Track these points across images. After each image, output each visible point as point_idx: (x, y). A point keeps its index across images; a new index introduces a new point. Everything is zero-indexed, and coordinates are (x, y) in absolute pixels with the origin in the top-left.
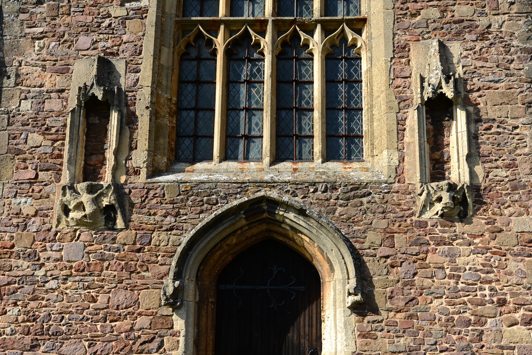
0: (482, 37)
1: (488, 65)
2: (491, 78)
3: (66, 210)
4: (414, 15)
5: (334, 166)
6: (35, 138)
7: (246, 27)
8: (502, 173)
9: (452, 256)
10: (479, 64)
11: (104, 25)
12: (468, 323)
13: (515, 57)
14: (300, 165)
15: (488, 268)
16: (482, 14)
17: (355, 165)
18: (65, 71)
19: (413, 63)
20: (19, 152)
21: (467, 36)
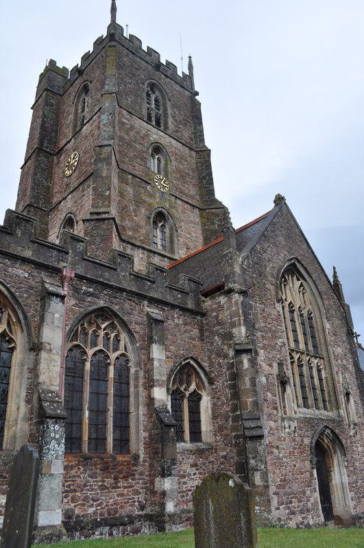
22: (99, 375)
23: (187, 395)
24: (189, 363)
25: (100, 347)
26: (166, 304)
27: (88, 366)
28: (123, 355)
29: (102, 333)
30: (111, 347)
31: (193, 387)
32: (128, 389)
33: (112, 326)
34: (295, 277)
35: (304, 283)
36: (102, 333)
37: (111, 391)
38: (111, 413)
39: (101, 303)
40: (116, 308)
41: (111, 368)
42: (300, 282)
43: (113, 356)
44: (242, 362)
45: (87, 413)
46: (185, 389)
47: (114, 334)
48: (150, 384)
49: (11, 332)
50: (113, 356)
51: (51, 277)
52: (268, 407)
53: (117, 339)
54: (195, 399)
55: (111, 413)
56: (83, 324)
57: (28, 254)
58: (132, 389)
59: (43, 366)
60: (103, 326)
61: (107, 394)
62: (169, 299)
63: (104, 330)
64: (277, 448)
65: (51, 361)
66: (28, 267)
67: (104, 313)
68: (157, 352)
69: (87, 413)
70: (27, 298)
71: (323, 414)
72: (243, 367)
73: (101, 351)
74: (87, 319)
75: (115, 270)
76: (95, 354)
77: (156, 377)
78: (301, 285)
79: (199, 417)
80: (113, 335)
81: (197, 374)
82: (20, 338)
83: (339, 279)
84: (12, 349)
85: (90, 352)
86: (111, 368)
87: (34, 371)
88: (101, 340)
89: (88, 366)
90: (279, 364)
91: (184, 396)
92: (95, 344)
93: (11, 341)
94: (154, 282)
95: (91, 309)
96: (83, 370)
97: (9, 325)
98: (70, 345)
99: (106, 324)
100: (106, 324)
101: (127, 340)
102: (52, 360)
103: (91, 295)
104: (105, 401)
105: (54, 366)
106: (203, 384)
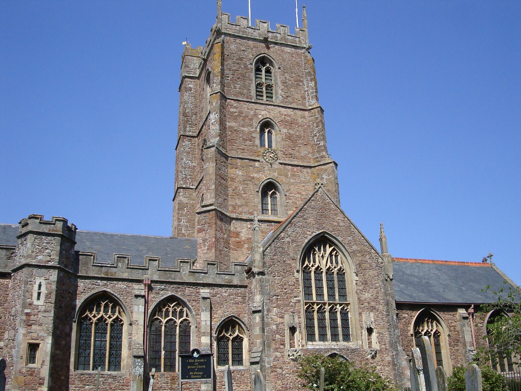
1: (379, 318)
2: (380, 322)
3: (289, 356)
4: (362, 305)
6: (278, 336)
7: (321, 305)
10: (377, 318)
11: (290, 304)
13: (384, 316)
16: (377, 305)
17: (350, 343)
18: (282, 317)
19: (363, 318)
20: (274, 340)
21: (374, 311)
22: (170, 332)
23: (231, 339)
24: (232, 319)
25: (170, 317)
27: (163, 328)
29: (171, 310)
30: (178, 317)
31: (237, 333)
32: (190, 338)
33: (178, 305)
34: (328, 246)
36: (171, 310)
37: (177, 340)
39: (170, 294)
40: (179, 295)
41: (178, 328)
43: (178, 321)
45: (163, 353)
46: (230, 335)
47: (179, 309)
49: (121, 316)
50: (178, 321)
51: (139, 284)
52: (275, 344)
53: (181, 312)
54: (238, 340)
55: (177, 352)
56: (160, 306)
57: (125, 276)
58: (191, 339)
59: (134, 332)
60: (172, 306)
61: (176, 342)
63: (173, 307)
64: (281, 368)
65: (138, 329)
67: (171, 299)
69: (163, 353)
70: (126, 299)
71: (329, 345)
72: (256, 321)
73: (171, 320)
75: (179, 272)
77: (203, 330)
79: (242, 351)
80: (178, 310)
81: (240, 325)
84: (122, 324)
85: (164, 321)
86: (178, 328)
87: (130, 334)
89: (163, 328)
91: (228, 339)
92: (167, 315)
93: (121, 321)
95: (162, 298)
96: (161, 331)
97: (119, 313)
99: (174, 304)
100: (174, 304)
101: (188, 311)
102: (139, 329)
105: (140, 331)
106: (244, 330)
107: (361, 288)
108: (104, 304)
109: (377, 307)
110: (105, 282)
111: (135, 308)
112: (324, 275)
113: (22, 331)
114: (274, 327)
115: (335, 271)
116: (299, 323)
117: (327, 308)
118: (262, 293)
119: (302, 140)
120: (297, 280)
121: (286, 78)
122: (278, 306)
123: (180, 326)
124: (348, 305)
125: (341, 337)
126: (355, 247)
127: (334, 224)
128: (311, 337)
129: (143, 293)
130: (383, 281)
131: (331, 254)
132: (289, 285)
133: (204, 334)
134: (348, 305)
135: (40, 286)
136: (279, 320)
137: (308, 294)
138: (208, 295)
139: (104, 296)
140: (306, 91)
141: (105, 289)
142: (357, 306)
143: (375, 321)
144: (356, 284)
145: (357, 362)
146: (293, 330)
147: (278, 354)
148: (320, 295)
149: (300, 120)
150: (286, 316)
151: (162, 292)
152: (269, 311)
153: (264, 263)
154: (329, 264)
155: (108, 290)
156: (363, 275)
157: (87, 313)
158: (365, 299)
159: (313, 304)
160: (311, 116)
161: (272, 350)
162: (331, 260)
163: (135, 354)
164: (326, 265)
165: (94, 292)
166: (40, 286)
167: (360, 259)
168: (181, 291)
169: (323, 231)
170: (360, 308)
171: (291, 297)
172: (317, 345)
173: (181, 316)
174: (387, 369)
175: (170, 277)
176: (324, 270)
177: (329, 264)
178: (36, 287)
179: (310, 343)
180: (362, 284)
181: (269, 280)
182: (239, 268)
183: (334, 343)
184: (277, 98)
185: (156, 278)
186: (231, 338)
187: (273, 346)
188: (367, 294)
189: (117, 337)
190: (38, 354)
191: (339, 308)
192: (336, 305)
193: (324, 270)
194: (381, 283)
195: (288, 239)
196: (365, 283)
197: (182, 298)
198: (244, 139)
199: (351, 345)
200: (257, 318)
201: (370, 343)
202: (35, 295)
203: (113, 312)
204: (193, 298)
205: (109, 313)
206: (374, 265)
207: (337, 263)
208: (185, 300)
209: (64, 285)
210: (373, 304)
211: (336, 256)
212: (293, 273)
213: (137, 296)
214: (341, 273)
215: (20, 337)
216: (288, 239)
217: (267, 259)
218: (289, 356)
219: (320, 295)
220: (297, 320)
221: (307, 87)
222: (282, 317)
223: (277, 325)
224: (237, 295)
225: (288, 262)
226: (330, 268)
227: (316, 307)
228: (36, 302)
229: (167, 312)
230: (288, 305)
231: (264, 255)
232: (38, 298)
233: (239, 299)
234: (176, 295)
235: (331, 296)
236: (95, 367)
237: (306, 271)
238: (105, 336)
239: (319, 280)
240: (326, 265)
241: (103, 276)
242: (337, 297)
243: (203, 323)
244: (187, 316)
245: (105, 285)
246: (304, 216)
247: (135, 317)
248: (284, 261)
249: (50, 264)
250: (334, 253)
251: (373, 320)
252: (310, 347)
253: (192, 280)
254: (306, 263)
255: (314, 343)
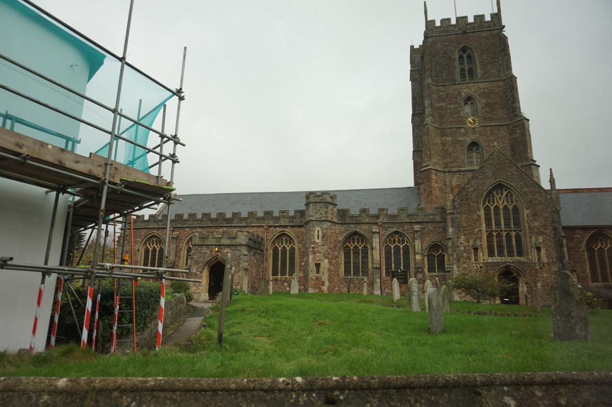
0: (546, 234)
5: (519, 258)
6: (465, 254)
8: (551, 260)
9: (542, 275)
12: (545, 286)
14: (513, 258)
15: (548, 276)
18: (468, 242)
25: (397, 244)
26: (423, 222)
27: (392, 250)
28: (406, 245)
29: (396, 239)
31: (440, 252)
33: (401, 236)
35: (510, 191)
36: (396, 239)
37: (402, 257)
38: (402, 265)
39: (395, 230)
41: (401, 250)
42: (507, 191)
43: (401, 246)
44: (449, 243)
45: (393, 265)
48: (415, 254)
50: (401, 246)
57: (367, 221)
62: (426, 219)
66: (368, 225)
67: (396, 233)
68: (418, 243)
69: (393, 265)
74: (391, 236)
76: (395, 246)
77: (416, 251)
78: (509, 192)
80: (401, 239)
82: (369, 246)
83: (554, 176)
84: (368, 250)
85: (392, 246)
86: (401, 250)
87: (372, 255)
88: (396, 241)
89: (392, 250)
90: (474, 240)
93: (367, 247)
94: (417, 215)
95: (390, 232)
96: (391, 252)
98: (385, 245)
103: (391, 227)
104: (400, 261)
107: (531, 219)
108: (356, 238)
109: (545, 231)
110: (355, 226)
111: (374, 240)
112: (501, 211)
113: (311, 257)
114: (462, 248)
115: (511, 207)
116: (481, 245)
117: (504, 234)
118: (453, 226)
119: (499, 105)
120: (479, 216)
121: (483, 58)
122: (465, 235)
123: (403, 249)
124: (520, 231)
125: (516, 254)
126: (526, 190)
127: (509, 174)
128: (491, 254)
129: (378, 231)
130: (550, 213)
131: (506, 196)
132: (473, 220)
133: (417, 253)
134: (520, 231)
135: (318, 231)
136: (466, 244)
137: (488, 224)
138: (419, 229)
139: (356, 233)
140: (500, 65)
141: (356, 230)
142: (527, 232)
143: (543, 241)
144: (527, 216)
145: (528, 271)
146: (476, 249)
147: (465, 266)
148: (498, 223)
149: (496, 90)
150: (471, 241)
151: (390, 229)
152: (458, 238)
153: (454, 206)
154: (505, 203)
155: (358, 230)
156: (533, 209)
157: (348, 244)
158: (535, 227)
159: (492, 231)
160: (506, 85)
161: (461, 263)
162: (507, 200)
163: (374, 266)
164: (503, 204)
165: (349, 232)
166: (318, 231)
167: (531, 197)
168: (402, 227)
169: (499, 180)
170: (530, 233)
171: (475, 228)
172: (497, 259)
173: (403, 242)
174: (553, 276)
175: (394, 220)
176: (501, 207)
177: (505, 203)
178: (316, 232)
179: (490, 258)
180: (532, 215)
181: (458, 217)
182: (440, 210)
183: (509, 258)
184: (477, 76)
185: (385, 221)
186: (436, 255)
187: (462, 260)
188: (536, 223)
189: (365, 257)
190: (321, 269)
191: (513, 234)
192: (511, 231)
193: (501, 207)
194: (549, 214)
195: (471, 189)
196: (535, 215)
197: (402, 232)
198: (451, 114)
199: (523, 259)
200: (450, 243)
201: (539, 258)
202: (316, 237)
203: (362, 243)
204: (410, 231)
205: (360, 243)
206: (543, 201)
207: (512, 202)
208: (405, 233)
209: (331, 229)
210: (541, 230)
211: (511, 196)
212: (476, 212)
213: (374, 233)
214: (516, 209)
215: (310, 260)
216: (471, 189)
217: (456, 203)
218: (473, 267)
219: (498, 223)
220: (478, 243)
221: (502, 61)
222: (468, 242)
223: (465, 247)
224: (439, 228)
225: (472, 204)
226: (506, 205)
227: (495, 234)
228: (317, 241)
229: (394, 240)
230: (472, 233)
231: (454, 201)
232: (318, 239)
233: (441, 230)
234: (399, 230)
235: (507, 224)
236: (354, 274)
237: (487, 209)
238: (359, 257)
239: (497, 214)
240: (503, 204)
241: (354, 222)
242: (512, 226)
243: (416, 247)
244: (407, 242)
245: (356, 227)
246: (484, 170)
247: (374, 245)
248: (469, 204)
249: (323, 219)
250: (509, 195)
251: (541, 241)
252: (489, 261)
253: (408, 221)
254: (487, 203)
255: (494, 258)
